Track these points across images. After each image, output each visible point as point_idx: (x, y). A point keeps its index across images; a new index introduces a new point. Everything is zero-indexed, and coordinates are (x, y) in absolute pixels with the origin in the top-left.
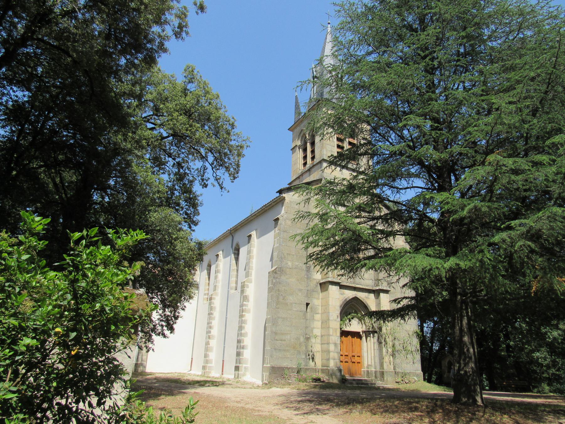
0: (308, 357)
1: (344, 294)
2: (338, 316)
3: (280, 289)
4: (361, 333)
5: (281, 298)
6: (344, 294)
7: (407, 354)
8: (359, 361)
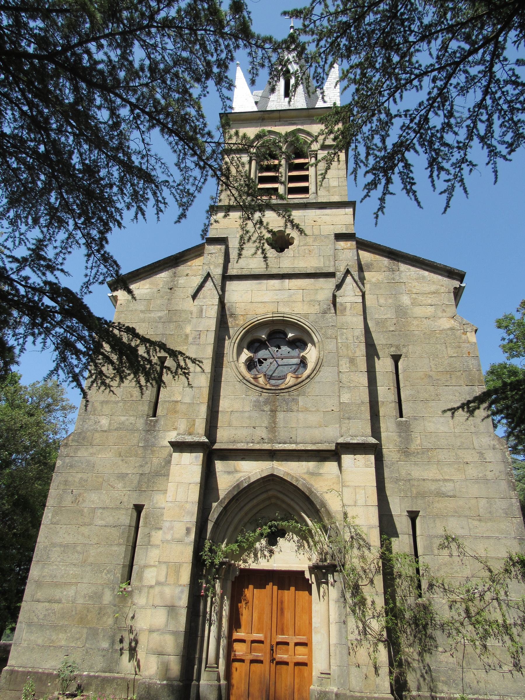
0: (118, 647)
1: (236, 471)
2: (188, 530)
3: (70, 479)
4: (307, 575)
5: (69, 498)
6: (236, 471)
7: (486, 635)
8: (300, 658)
